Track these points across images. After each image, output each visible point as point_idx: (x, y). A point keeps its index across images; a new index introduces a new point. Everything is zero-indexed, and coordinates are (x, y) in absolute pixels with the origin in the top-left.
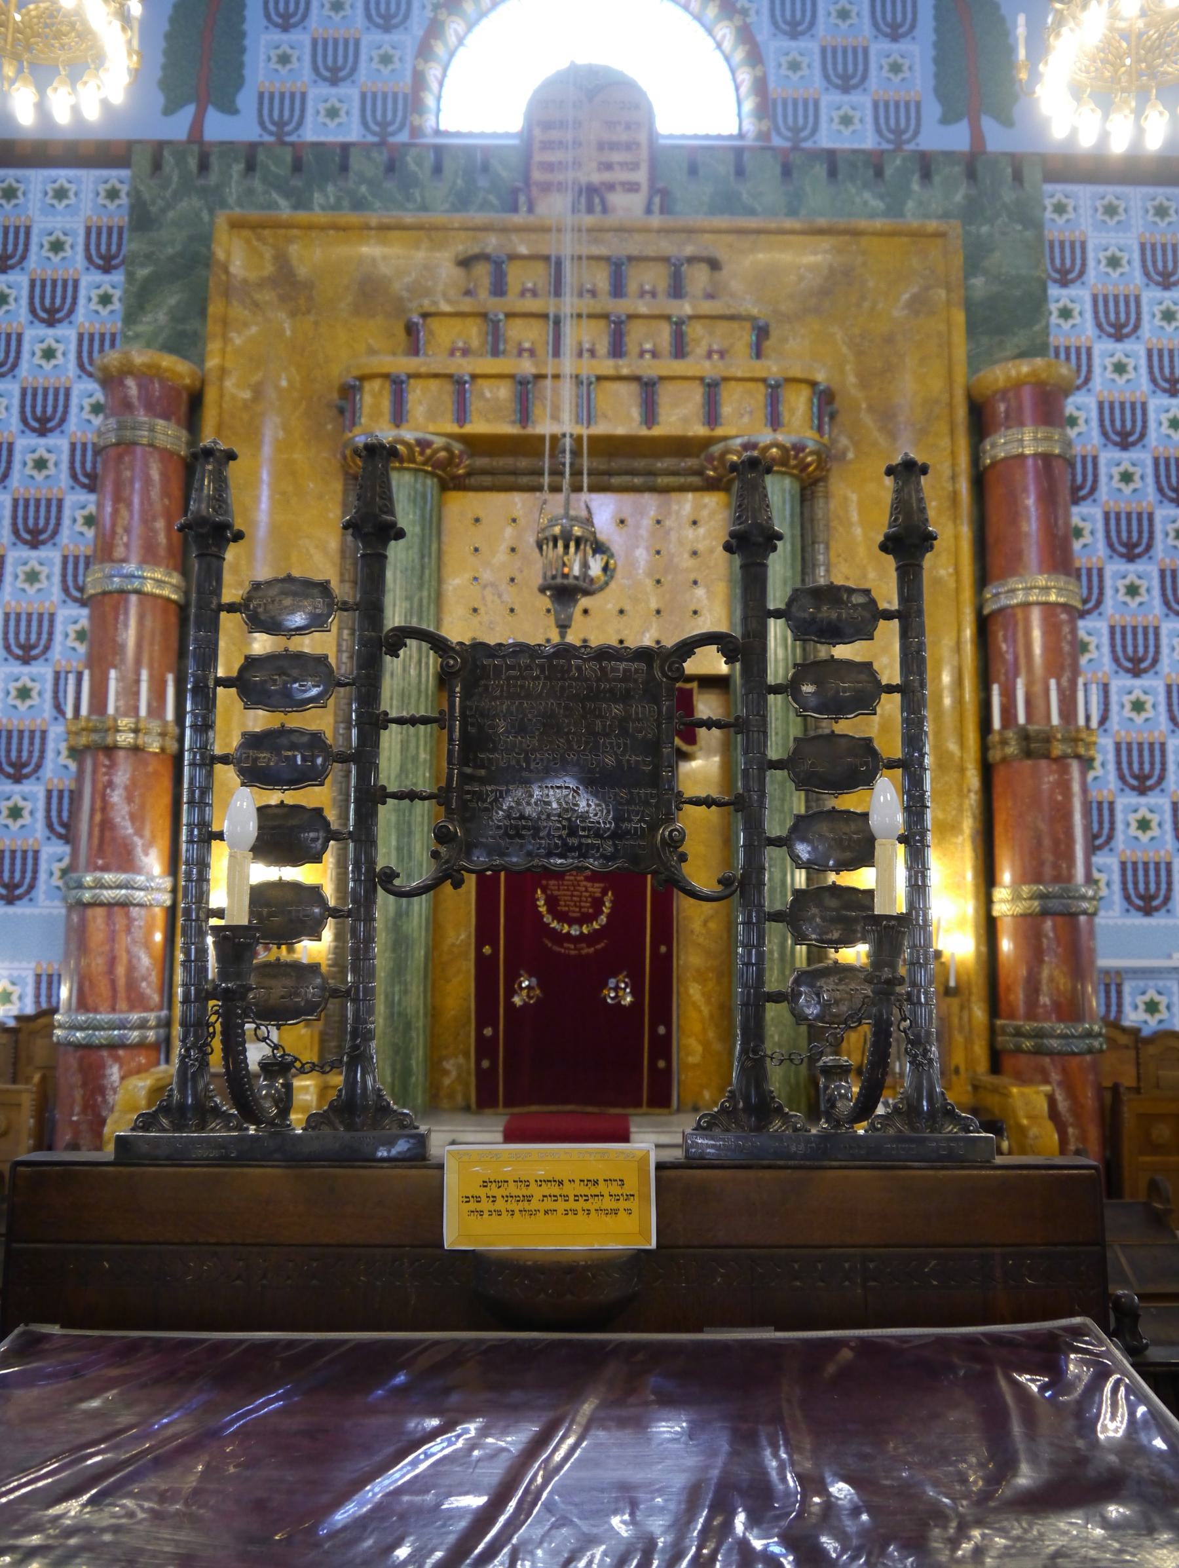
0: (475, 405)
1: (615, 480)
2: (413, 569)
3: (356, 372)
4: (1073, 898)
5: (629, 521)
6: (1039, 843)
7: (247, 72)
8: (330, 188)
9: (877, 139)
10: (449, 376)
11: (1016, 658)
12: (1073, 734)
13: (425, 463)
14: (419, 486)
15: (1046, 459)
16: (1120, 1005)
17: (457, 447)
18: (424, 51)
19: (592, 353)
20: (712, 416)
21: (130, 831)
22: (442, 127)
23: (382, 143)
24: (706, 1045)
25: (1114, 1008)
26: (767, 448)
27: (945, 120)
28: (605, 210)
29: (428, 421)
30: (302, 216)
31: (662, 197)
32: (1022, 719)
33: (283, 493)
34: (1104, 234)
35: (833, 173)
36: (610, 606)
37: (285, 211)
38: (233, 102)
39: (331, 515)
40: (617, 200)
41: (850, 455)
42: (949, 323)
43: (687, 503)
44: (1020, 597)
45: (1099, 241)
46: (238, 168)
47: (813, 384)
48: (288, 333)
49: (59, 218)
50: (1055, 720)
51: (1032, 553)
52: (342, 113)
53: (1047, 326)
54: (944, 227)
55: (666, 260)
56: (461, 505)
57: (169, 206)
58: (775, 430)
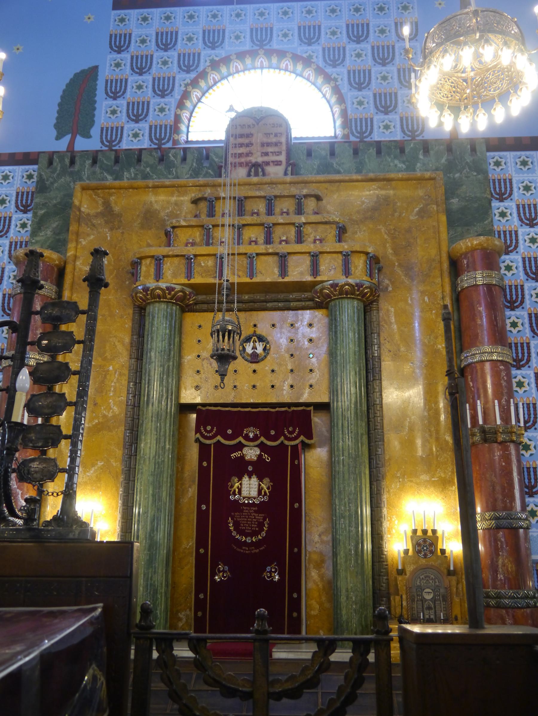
0: (196, 269)
1: (269, 305)
2: (165, 351)
3: (138, 256)
4: (514, 519)
5: (278, 325)
6: (494, 489)
7: (96, 119)
8: (132, 170)
10: (184, 256)
11: (478, 389)
12: (509, 430)
13: (171, 299)
14: (169, 310)
15: (489, 286)
17: (188, 290)
18: (181, 105)
19: (256, 242)
20: (315, 270)
21: (15, 486)
22: (189, 139)
23: (159, 148)
24: (321, 604)
26: (343, 286)
28: (264, 174)
29: (173, 277)
30: (117, 183)
31: (293, 167)
32: (481, 422)
34: (521, 175)
35: (379, 152)
36: (267, 368)
37: (110, 181)
38: (89, 132)
39: (127, 326)
40: (270, 169)
41: (390, 289)
42: (438, 222)
43: (307, 315)
44: (477, 358)
46: (89, 162)
47: (367, 254)
48: (109, 238)
49: (4, 189)
50: (499, 422)
51: (485, 334)
52: (140, 135)
53: (492, 221)
54: (433, 175)
55: (294, 196)
57: (55, 181)
58: (347, 277)
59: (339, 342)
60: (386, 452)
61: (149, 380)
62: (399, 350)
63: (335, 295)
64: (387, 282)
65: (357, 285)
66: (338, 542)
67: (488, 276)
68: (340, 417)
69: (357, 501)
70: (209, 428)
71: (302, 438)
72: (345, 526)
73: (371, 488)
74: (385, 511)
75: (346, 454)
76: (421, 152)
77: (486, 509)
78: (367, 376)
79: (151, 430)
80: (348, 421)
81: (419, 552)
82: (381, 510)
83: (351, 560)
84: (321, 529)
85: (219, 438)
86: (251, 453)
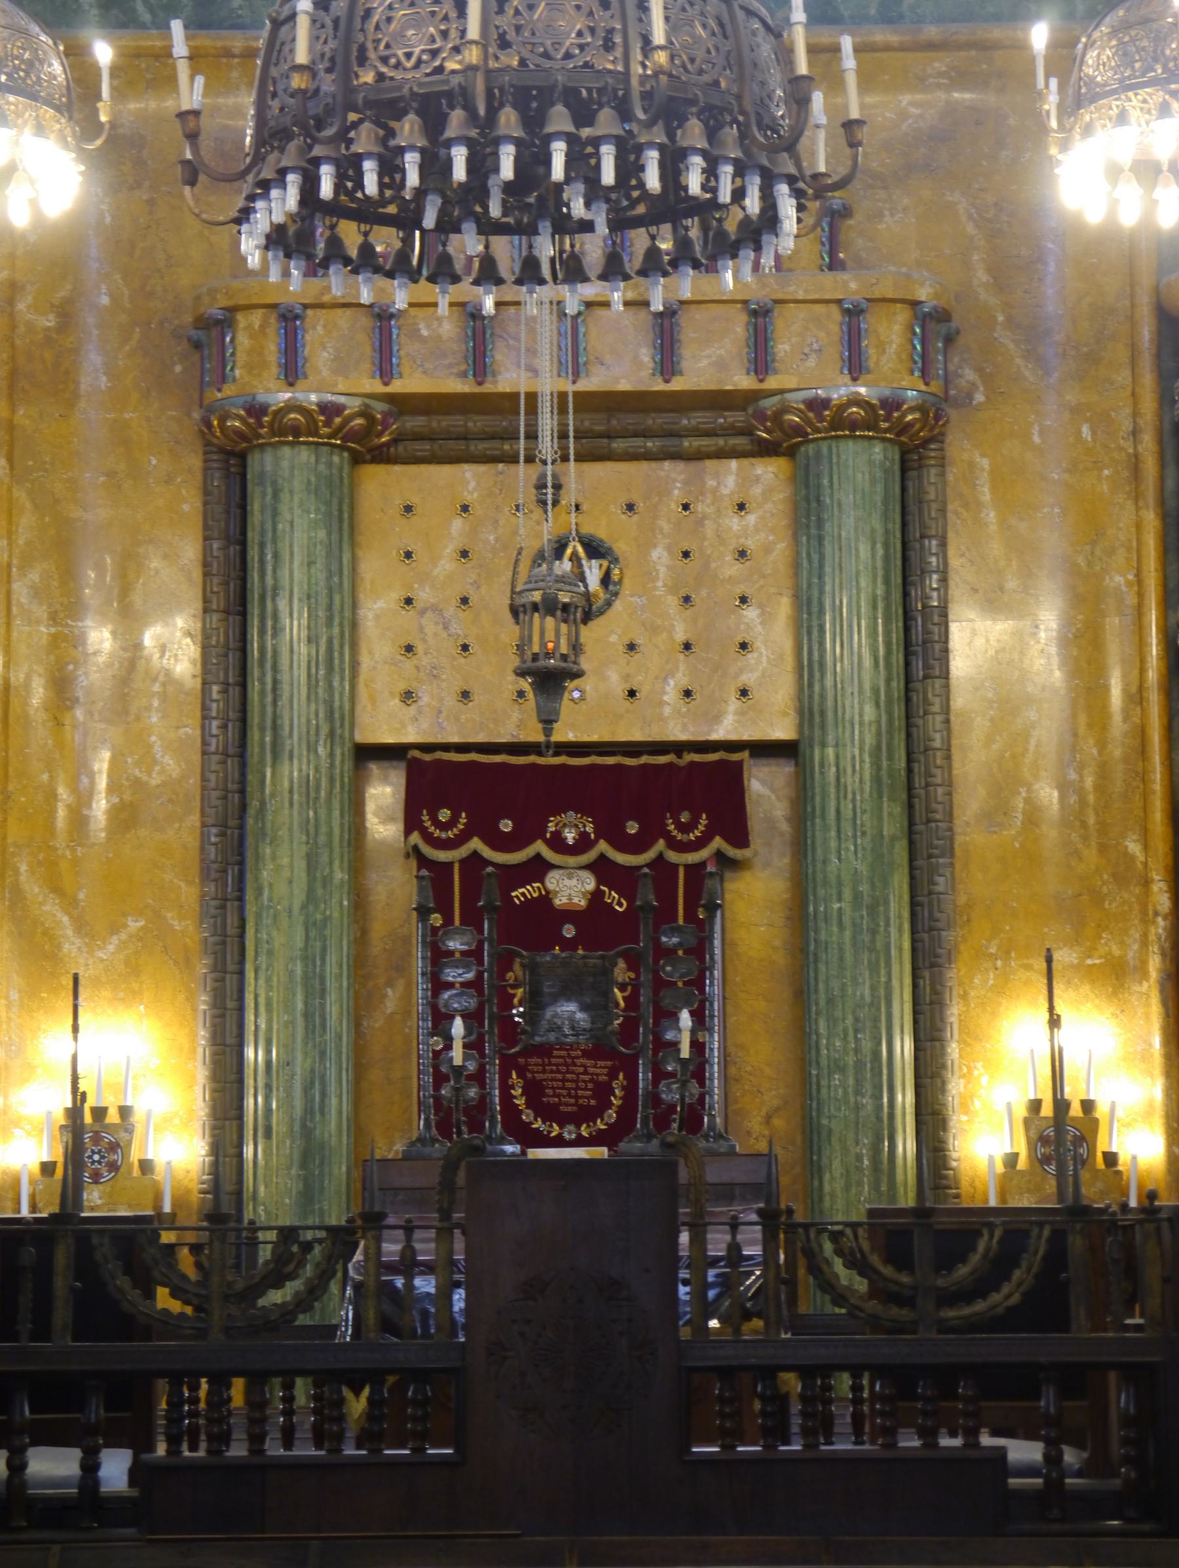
0: (405, 349)
1: (618, 445)
5: (640, 506)
14: (322, 467)
20: (761, 358)
26: (842, 407)
29: (337, 376)
33: (111, 474)
36: (613, 638)
39: (186, 507)
41: (979, 398)
43: (729, 476)
47: (915, 304)
56: (383, 485)
58: (855, 379)
59: (828, 569)
60: (960, 886)
61: (275, 682)
62: (1002, 589)
63: (818, 431)
64: (970, 375)
65: (884, 403)
66: (824, 1135)
68: (832, 790)
69: (875, 1022)
70: (444, 815)
71: (718, 842)
72: (846, 1093)
73: (915, 986)
74: (954, 1050)
75: (847, 893)
78: (907, 664)
79: (290, 830)
80: (854, 800)
81: (1045, 1160)
82: (943, 1048)
83: (860, 1184)
84: (771, 1098)
85: (476, 844)
86: (570, 887)
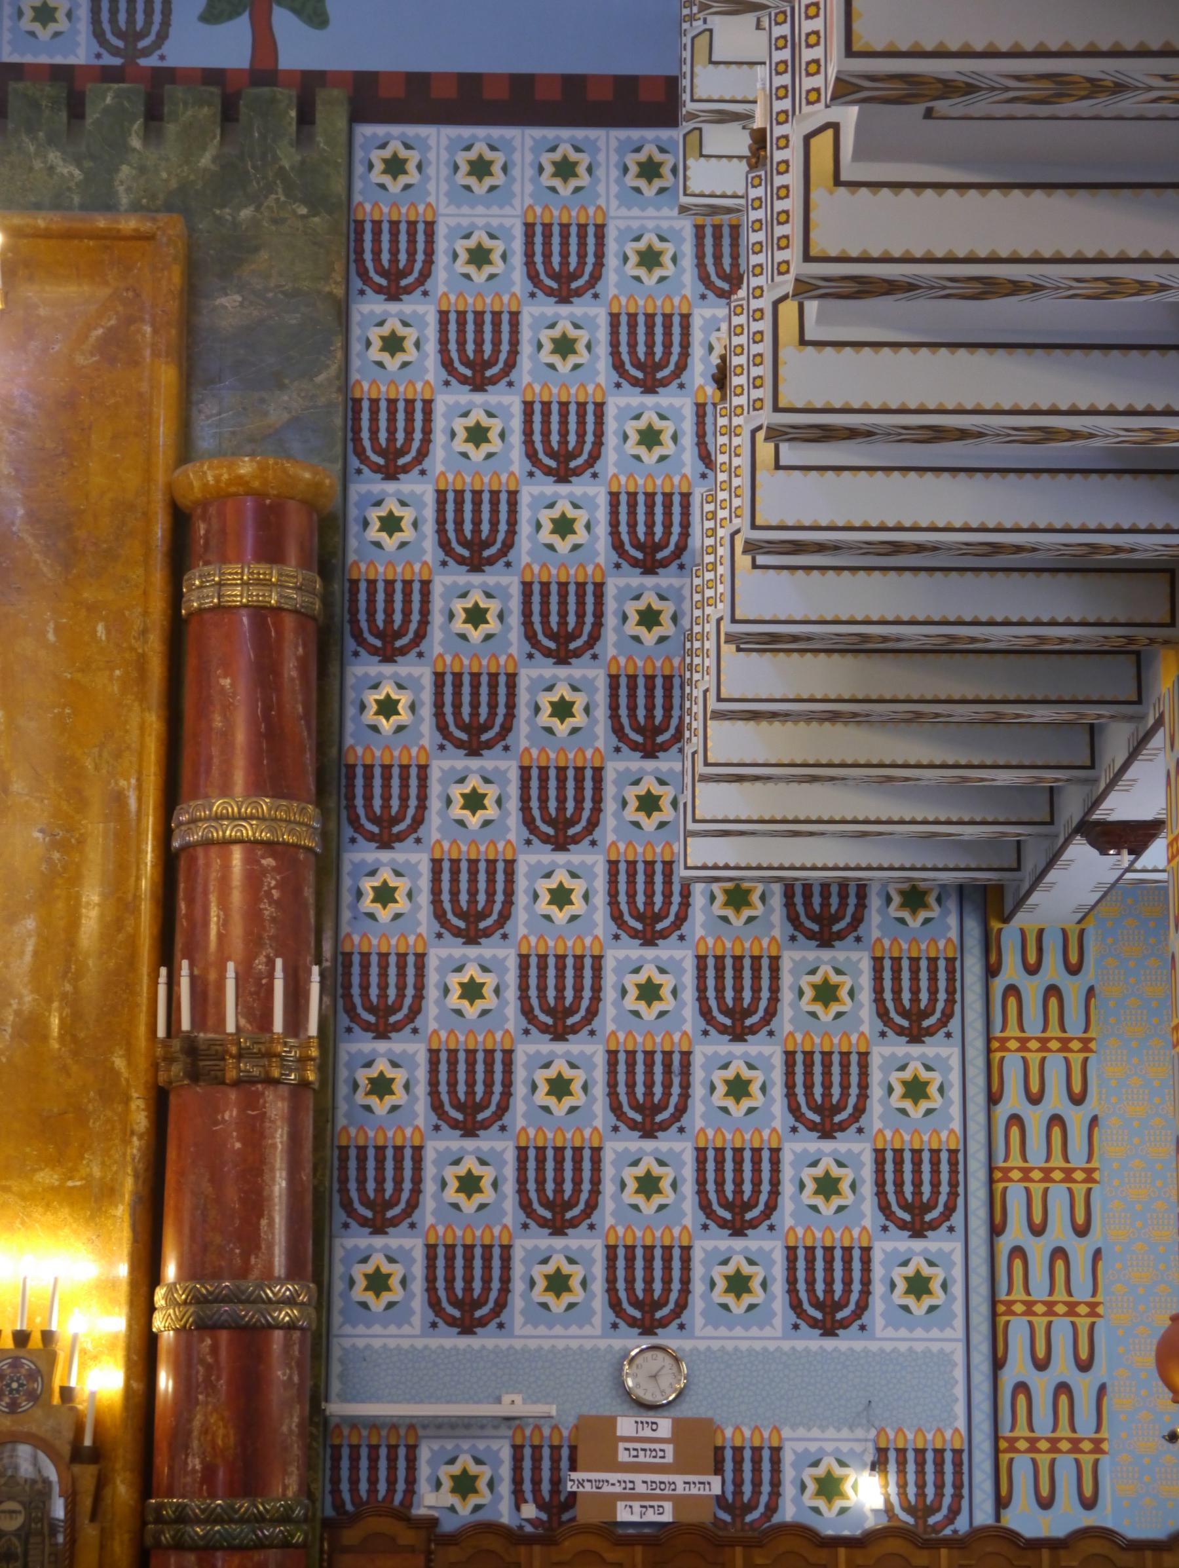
9: (97, 48)
15: (260, 612)
16: (411, 1481)
25: (401, 1486)
27: (211, 16)
32: (186, 1025)
34: (465, 210)
45: (456, 219)
67: (259, 583)
76: (138, 124)
77: (190, 1272)
